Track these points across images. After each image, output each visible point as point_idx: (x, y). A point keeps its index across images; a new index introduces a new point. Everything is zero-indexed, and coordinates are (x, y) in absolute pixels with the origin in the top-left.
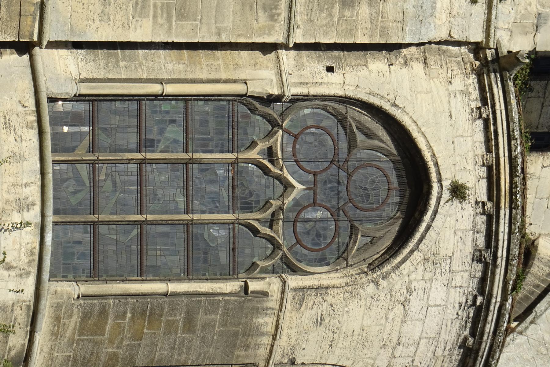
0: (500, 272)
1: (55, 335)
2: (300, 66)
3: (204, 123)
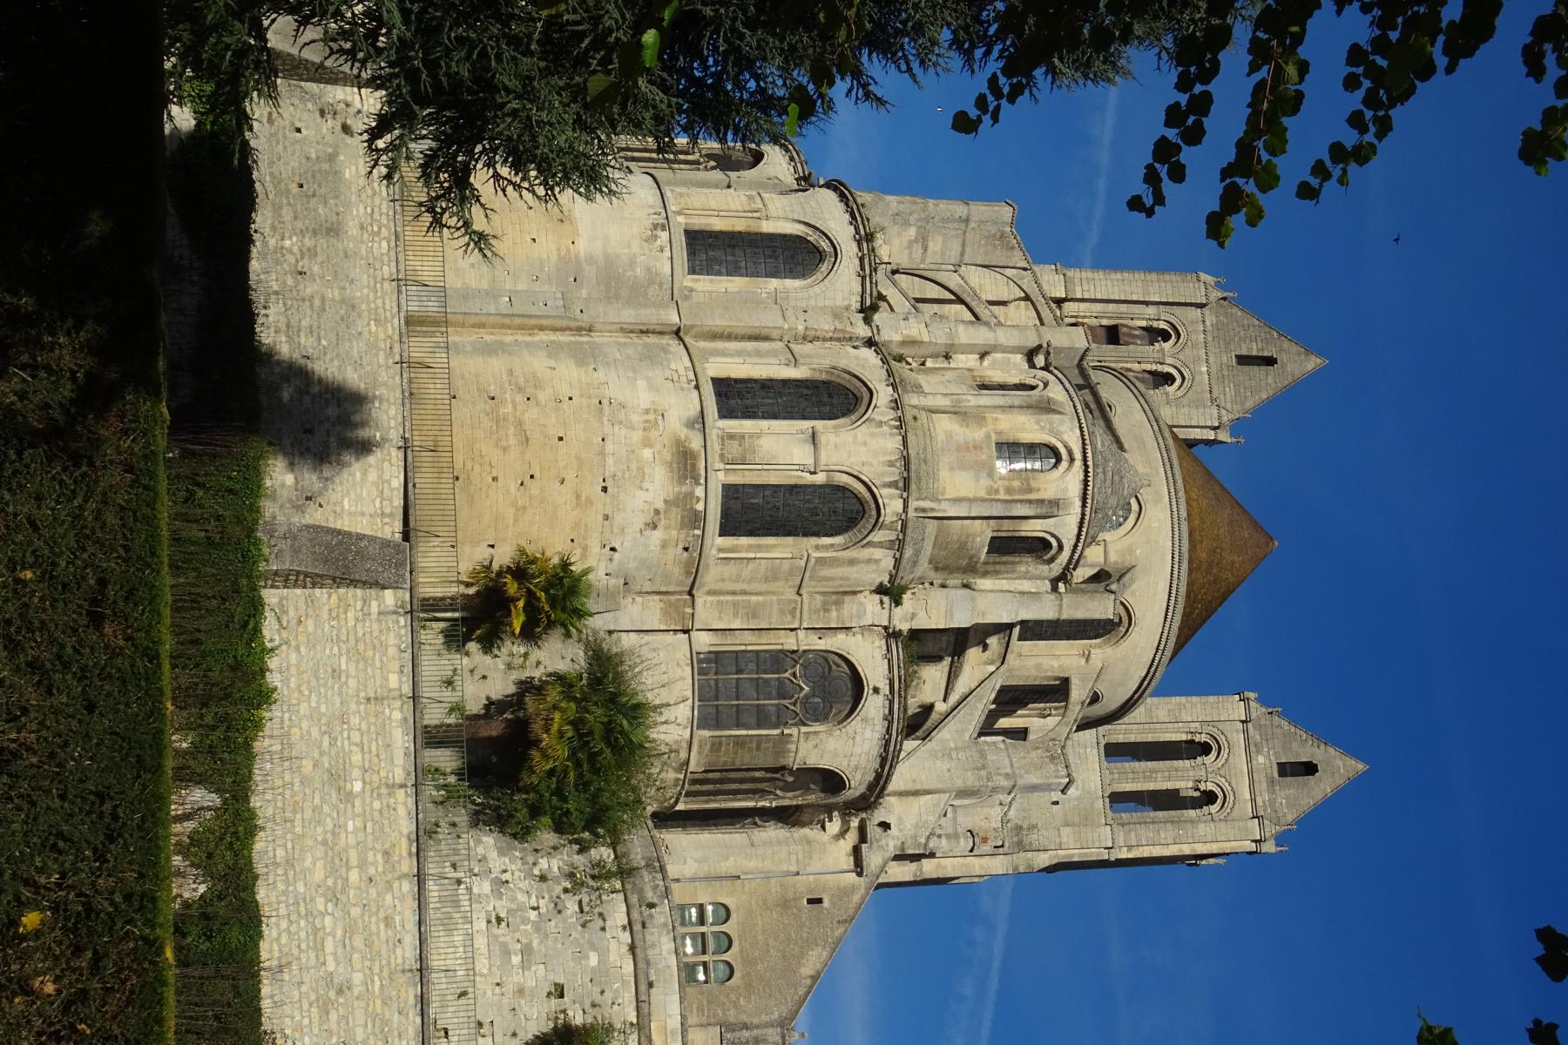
0: (895, 725)
1: (700, 753)
2: (807, 637)
3: (765, 662)
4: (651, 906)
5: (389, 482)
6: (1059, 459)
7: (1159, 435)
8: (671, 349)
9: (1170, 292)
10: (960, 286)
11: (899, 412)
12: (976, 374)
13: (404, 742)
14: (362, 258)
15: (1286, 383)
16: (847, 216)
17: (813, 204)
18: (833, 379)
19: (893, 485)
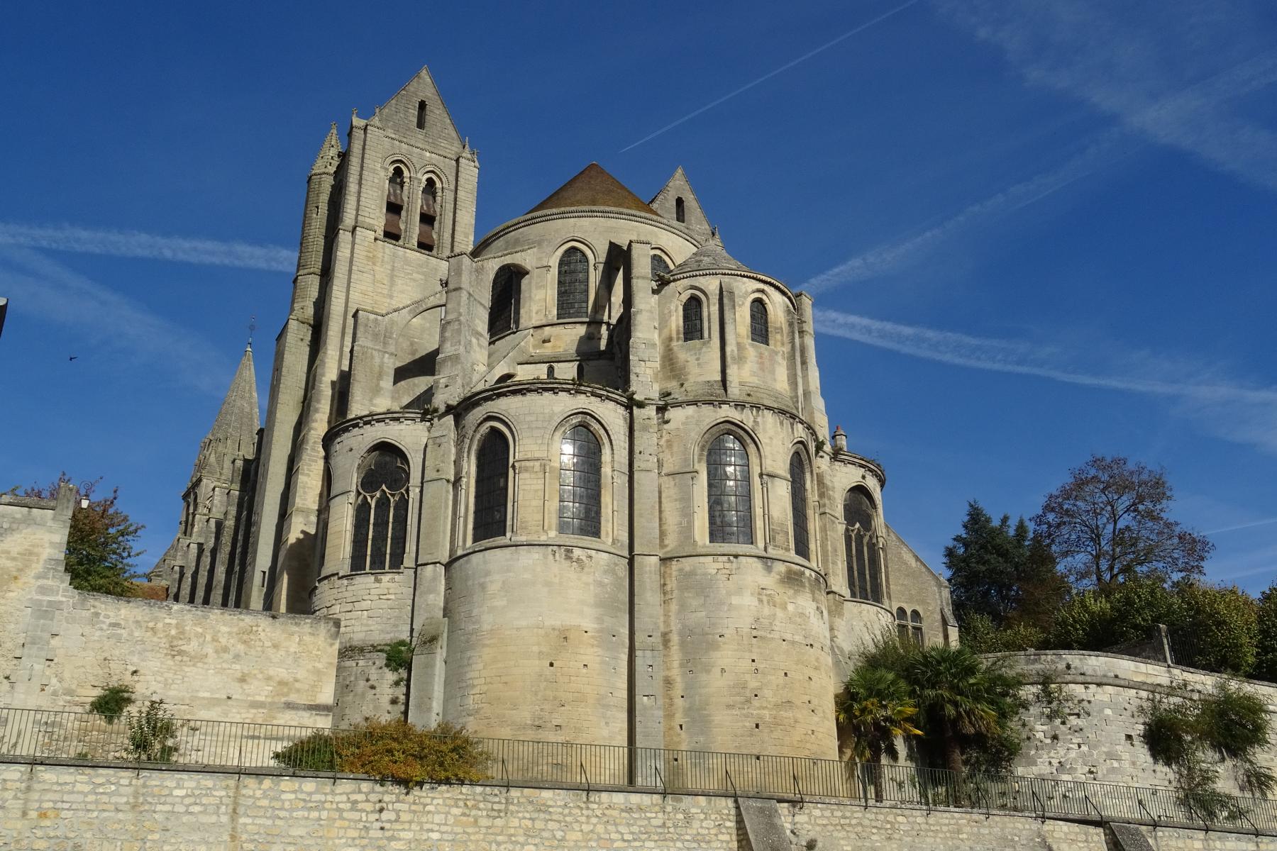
4: (1068, 667)
5: (1066, 834)
7: (605, 214)
8: (687, 569)
9: (374, 154)
10: (411, 310)
11: (747, 405)
12: (674, 335)
13: (1232, 841)
14: (914, 841)
15: (440, 102)
16: (546, 394)
17: (528, 418)
18: (707, 447)
19: (792, 425)
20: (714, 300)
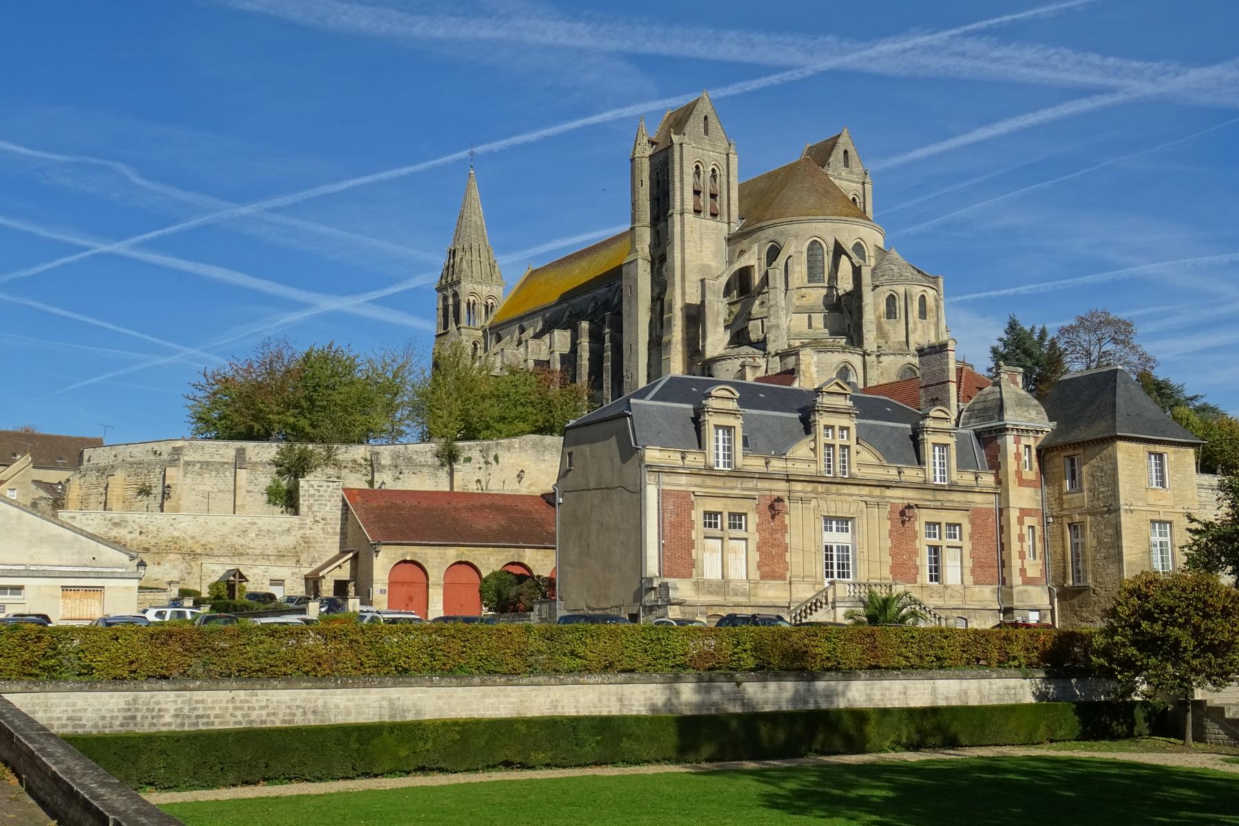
6: (923, 296)
20: (903, 298)
